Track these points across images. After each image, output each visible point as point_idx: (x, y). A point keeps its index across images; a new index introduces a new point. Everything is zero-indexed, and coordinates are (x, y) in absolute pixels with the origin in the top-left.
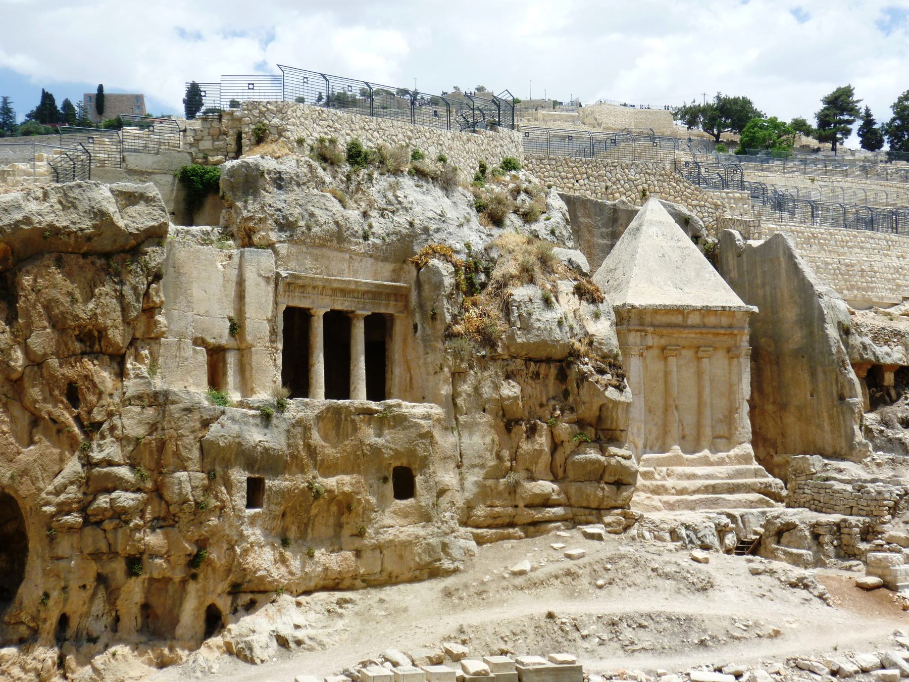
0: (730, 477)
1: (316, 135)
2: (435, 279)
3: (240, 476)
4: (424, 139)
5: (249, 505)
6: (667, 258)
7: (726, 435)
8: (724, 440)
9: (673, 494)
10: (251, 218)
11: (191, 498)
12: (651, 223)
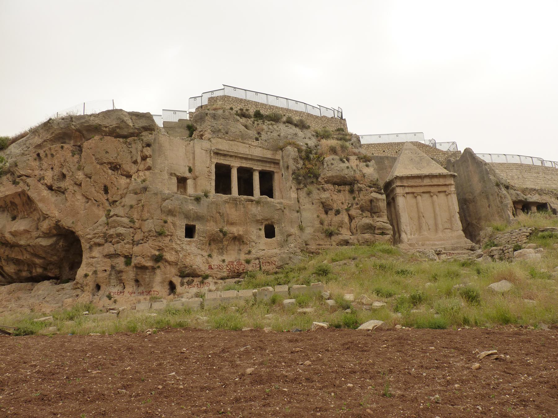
1: (239, 108)
2: (287, 153)
3: (181, 224)
5: (186, 237)
7: (450, 227)
10: (202, 131)
11: (153, 230)
12: (406, 149)
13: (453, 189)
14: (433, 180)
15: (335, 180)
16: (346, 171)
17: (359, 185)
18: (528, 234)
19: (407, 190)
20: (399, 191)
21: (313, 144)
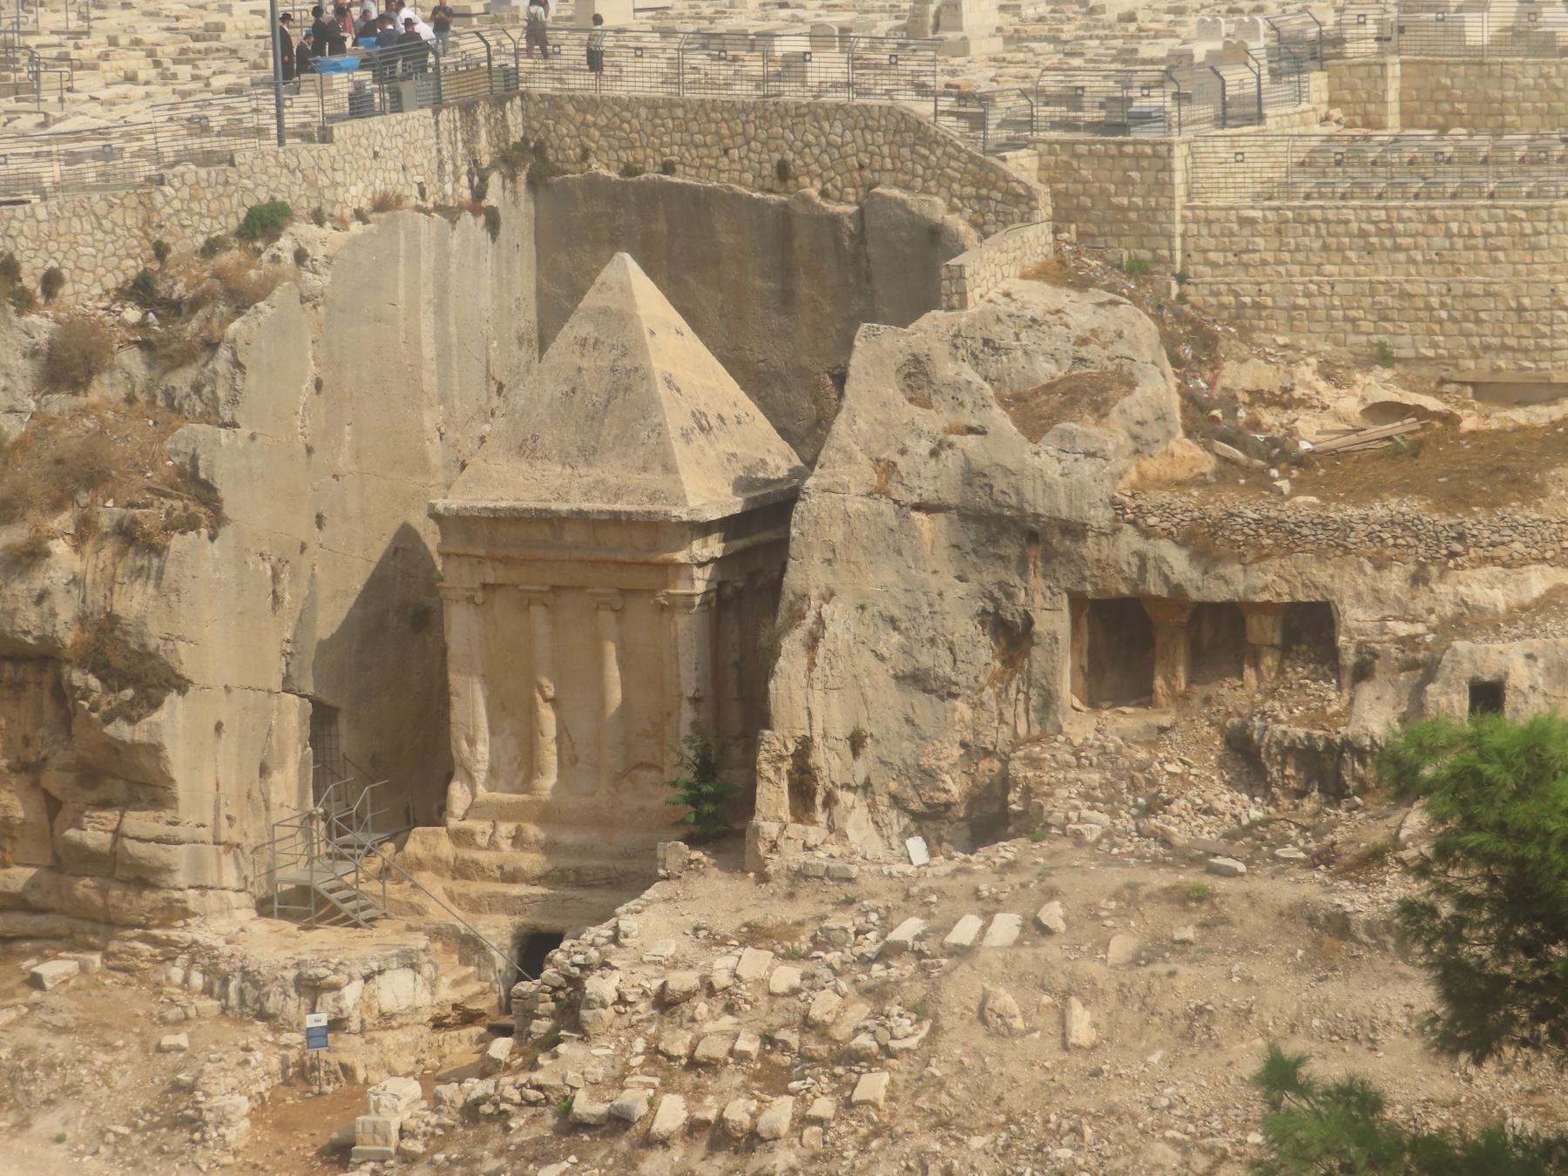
6: (579, 394)
8: (653, 774)
9: (496, 880)
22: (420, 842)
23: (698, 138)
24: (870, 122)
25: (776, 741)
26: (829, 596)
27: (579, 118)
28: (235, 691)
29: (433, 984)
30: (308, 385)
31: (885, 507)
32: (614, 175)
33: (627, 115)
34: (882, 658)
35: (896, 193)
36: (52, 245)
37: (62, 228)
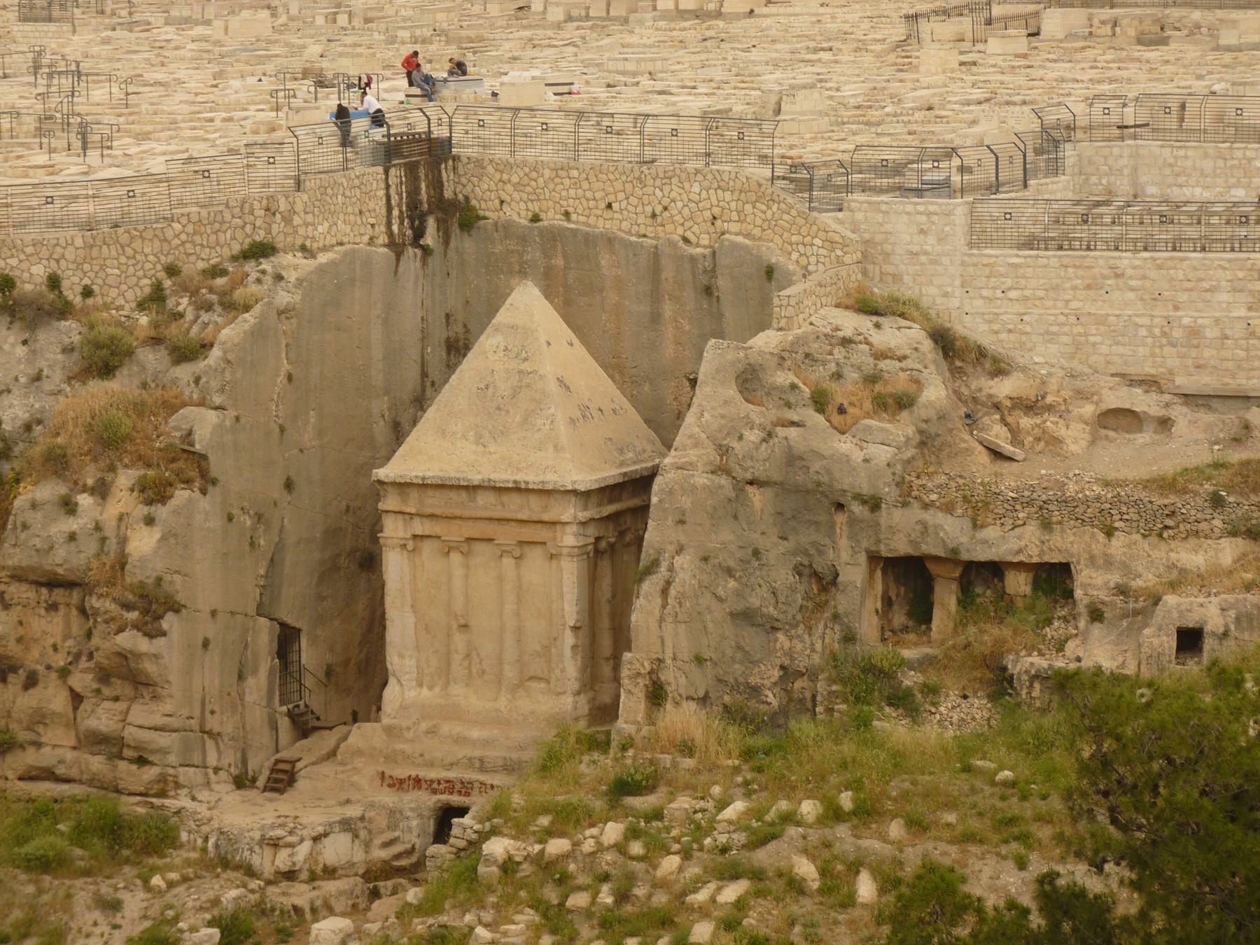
0: (521, 748)
4: (22, 257)
6: (491, 390)
8: (543, 685)
13: (569, 539)
14: (506, 498)
15: (32, 577)
16: (60, 554)
17: (94, 599)
18: (462, 844)
19: (419, 527)
20: (393, 530)
21: (24, 416)
22: (363, 735)
23: (589, 194)
24: (722, 184)
25: (635, 661)
26: (680, 550)
27: (498, 176)
28: (220, 616)
29: (367, 845)
30: (281, 378)
31: (724, 481)
32: (525, 222)
33: (534, 175)
34: (720, 599)
35: (740, 239)
36: (86, 267)
37: (95, 252)
